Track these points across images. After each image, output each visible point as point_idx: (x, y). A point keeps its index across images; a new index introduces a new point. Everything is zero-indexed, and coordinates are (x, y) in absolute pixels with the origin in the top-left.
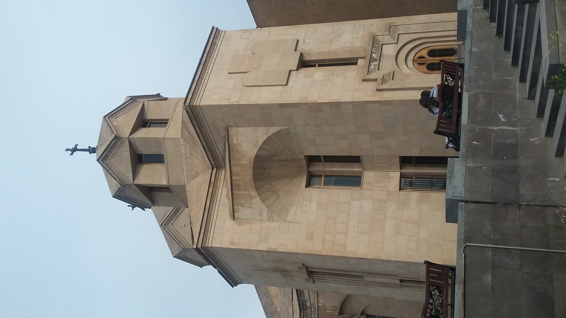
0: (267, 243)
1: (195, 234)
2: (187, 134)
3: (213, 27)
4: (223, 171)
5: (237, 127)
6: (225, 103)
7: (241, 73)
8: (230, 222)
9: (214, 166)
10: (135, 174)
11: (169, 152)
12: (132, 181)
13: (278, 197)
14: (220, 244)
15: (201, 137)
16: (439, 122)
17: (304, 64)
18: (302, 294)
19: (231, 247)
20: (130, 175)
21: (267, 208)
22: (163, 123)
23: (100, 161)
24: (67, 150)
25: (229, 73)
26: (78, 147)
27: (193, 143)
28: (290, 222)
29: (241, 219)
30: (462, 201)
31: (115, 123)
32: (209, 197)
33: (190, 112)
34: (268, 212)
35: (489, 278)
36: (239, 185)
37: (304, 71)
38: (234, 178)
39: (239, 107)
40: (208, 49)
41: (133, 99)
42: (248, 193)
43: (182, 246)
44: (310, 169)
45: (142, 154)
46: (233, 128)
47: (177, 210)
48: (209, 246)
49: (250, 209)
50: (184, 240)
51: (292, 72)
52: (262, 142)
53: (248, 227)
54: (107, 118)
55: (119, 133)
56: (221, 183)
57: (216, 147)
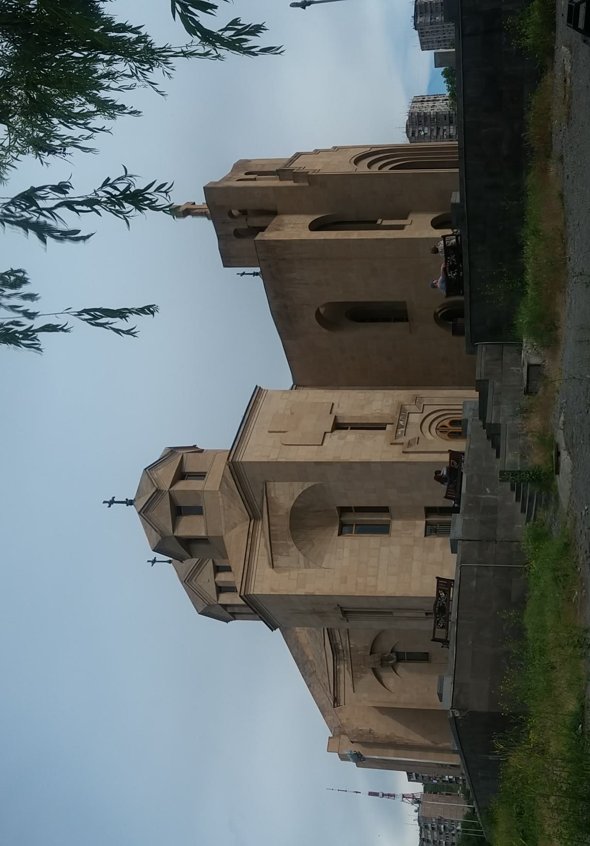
0: (305, 588)
1: (237, 583)
2: (226, 487)
4: (261, 522)
5: (275, 481)
6: (265, 460)
8: (269, 571)
9: (252, 517)
10: (174, 526)
11: (207, 504)
13: (313, 545)
14: (262, 591)
15: (241, 490)
16: (447, 491)
19: (272, 593)
20: (170, 527)
21: (304, 555)
22: (201, 476)
23: (142, 513)
24: (105, 502)
25: (269, 432)
28: (325, 568)
29: (280, 567)
30: (460, 540)
32: (249, 547)
33: (232, 468)
34: (304, 559)
35: (474, 583)
38: (272, 528)
42: (285, 542)
44: (342, 519)
45: (180, 507)
48: (251, 593)
49: (287, 557)
52: (297, 496)
53: (287, 574)
54: (147, 470)
55: (159, 486)
56: (259, 534)
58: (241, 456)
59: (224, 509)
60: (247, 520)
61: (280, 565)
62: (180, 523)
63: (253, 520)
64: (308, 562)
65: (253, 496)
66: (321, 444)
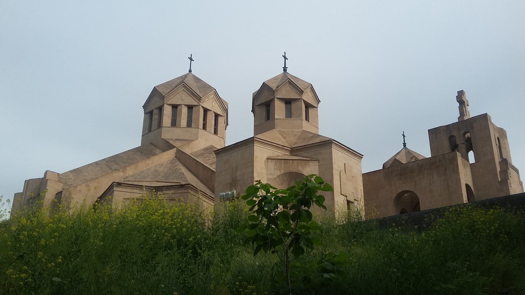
4: (289, 154)
5: (318, 166)
9: (292, 149)
11: (293, 121)
12: (277, 97)
13: (279, 185)
15: (312, 145)
17: (349, 202)
18: (168, 189)
20: (280, 96)
21: (275, 178)
22: (307, 119)
25: (345, 164)
26: (286, 60)
27: (305, 139)
29: (268, 163)
31: (308, 91)
32: (278, 146)
34: (272, 178)
36: (287, 164)
37: (346, 202)
38: (291, 161)
39: (332, 168)
40: (354, 152)
41: (319, 101)
42: (283, 168)
43: (166, 96)
46: (318, 163)
47: (195, 96)
48: (255, 144)
50: (170, 98)
51: (346, 197)
53: (264, 167)
54: (311, 86)
56: (283, 152)
57: (305, 152)
58: (335, 148)
59: (292, 132)
60: (290, 146)
61: (269, 163)
62: (282, 103)
63: (290, 150)
64: (271, 180)
65: (308, 151)
66: (342, 194)
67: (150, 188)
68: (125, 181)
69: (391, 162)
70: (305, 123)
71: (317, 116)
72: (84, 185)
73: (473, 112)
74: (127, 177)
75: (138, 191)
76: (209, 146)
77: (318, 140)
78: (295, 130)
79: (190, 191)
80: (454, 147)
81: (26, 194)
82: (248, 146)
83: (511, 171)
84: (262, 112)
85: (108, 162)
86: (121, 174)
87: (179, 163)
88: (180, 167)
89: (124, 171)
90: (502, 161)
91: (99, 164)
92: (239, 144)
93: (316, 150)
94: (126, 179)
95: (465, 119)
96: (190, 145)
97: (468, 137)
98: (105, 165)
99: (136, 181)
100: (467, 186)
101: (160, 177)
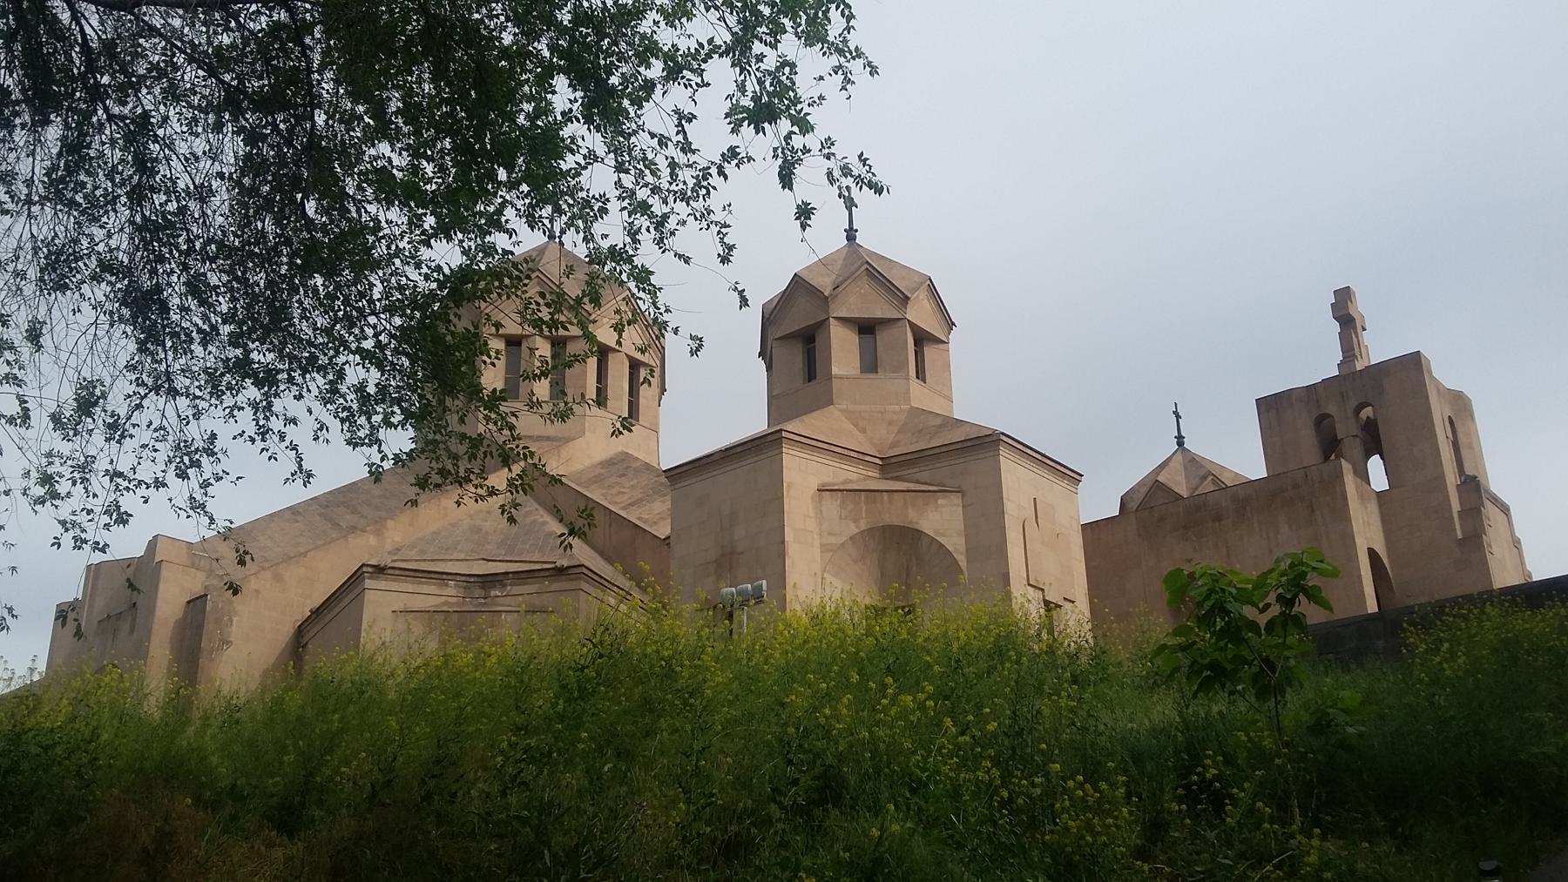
3: (1082, 476)
4: (877, 476)
5: (964, 507)
7: (1036, 517)
8: (814, 484)
9: (887, 461)
10: (844, 320)
11: (884, 382)
12: (834, 315)
13: (855, 562)
15: (944, 449)
22: (921, 374)
26: (854, 208)
27: (920, 431)
29: (820, 502)
31: (921, 297)
32: (846, 452)
33: (988, 439)
36: (875, 502)
48: (784, 450)
53: (812, 514)
54: (929, 282)
57: (922, 468)
60: (879, 452)
65: (931, 467)
67: (467, 579)
68: (395, 561)
69: (1144, 490)
70: (915, 384)
71: (947, 366)
72: (268, 574)
73: (1379, 348)
74: (399, 550)
75: (433, 589)
76: (615, 454)
77: (957, 436)
78: (890, 408)
79: (584, 586)
80: (1330, 446)
81: (91, 606)
82: (765, 456)
83: (1490, 510)
84: (793, 357)
85: (327, 506)
86: (372, 540)
87: (536, 506)
88: (542, 516)
89: (378, 533)
90: (1462, 483)
91: (299, 513)
92: (739, 449)
93: (952, 462)
94: (395, 554)
95: (1359, 368)
96: (564, 453)
97: (1368, 417)
98: (320, 515)
99: (425, 560)
100: (1372, 553)
101: (490, 547)
